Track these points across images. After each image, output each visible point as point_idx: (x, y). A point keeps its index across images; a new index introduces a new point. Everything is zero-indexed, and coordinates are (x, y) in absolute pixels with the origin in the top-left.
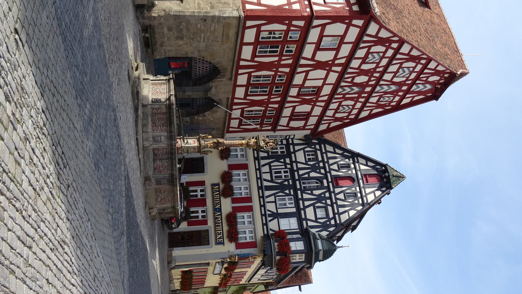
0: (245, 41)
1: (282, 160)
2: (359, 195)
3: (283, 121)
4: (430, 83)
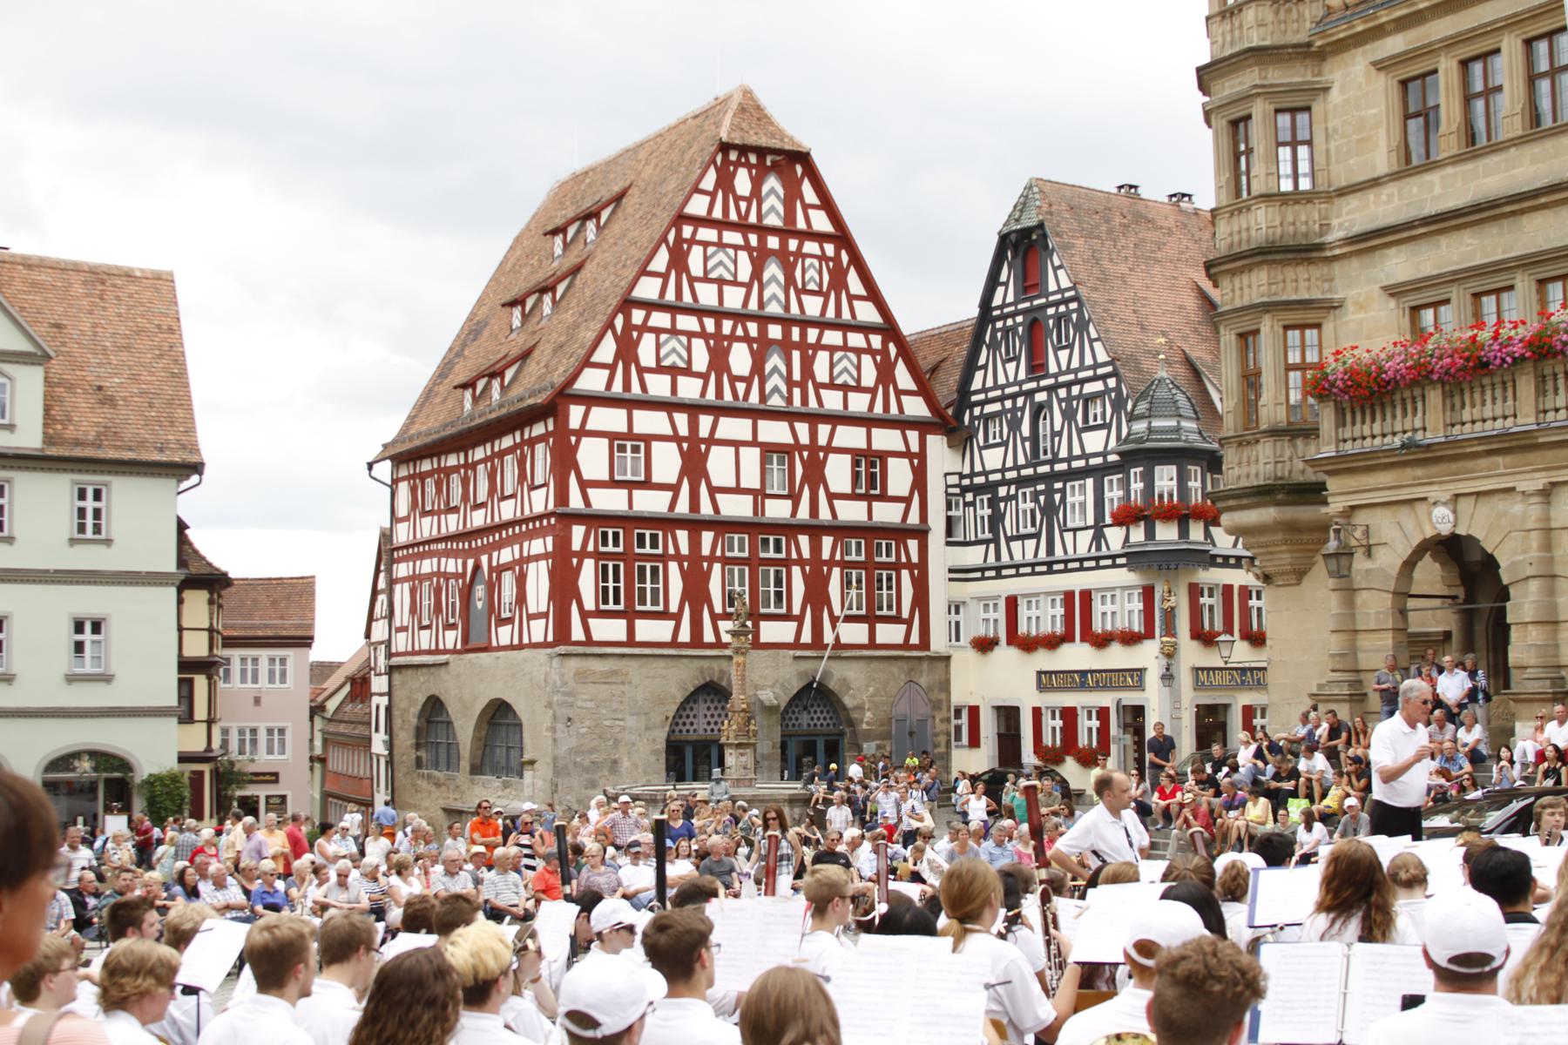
0: (622, 636)
1: (1002, 505)
2: (1062, 309)
3: (888, 514)
4: (757, 184)
